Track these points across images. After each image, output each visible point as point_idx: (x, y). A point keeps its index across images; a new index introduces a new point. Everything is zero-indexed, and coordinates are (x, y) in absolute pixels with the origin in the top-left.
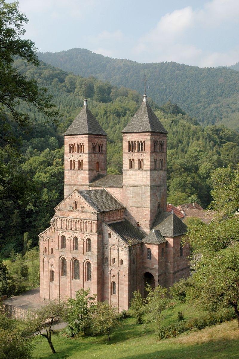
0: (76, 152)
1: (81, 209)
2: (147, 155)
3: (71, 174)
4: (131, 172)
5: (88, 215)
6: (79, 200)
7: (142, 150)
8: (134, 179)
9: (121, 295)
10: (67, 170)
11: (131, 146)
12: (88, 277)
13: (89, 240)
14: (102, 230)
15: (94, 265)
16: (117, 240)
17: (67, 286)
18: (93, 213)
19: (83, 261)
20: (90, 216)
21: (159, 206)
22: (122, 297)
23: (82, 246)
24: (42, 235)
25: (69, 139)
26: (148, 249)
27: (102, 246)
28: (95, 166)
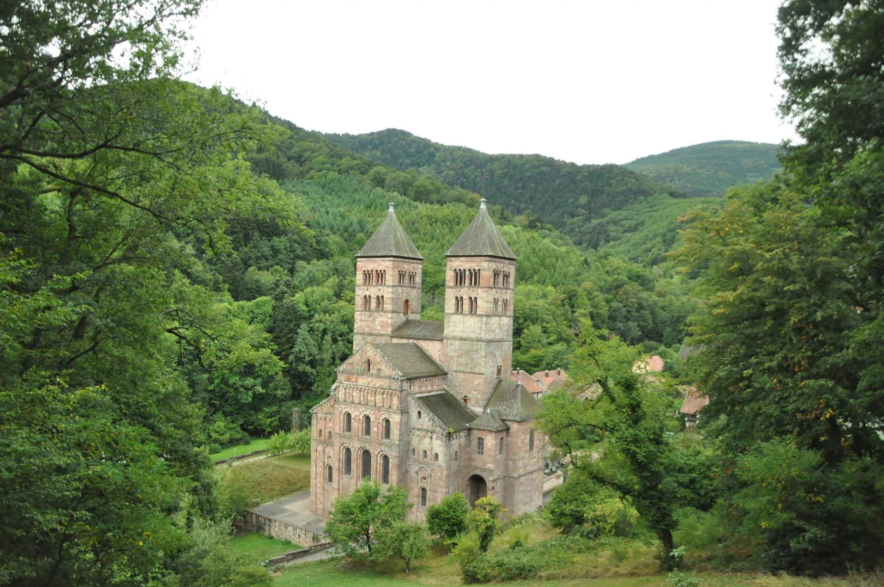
1: (376, 372)
4: (458, 318)
5: (387, 381)
7: (475, 284)
8: (460, 328)
11: (460, 277)
13: (388, 421)
14: (407, 406)
16: (431, 423)
21: (499, 371)
23: (375, 429)
24: (315, 411)
26: (479, 438)
27: (407, 430)
28: (402, 306)
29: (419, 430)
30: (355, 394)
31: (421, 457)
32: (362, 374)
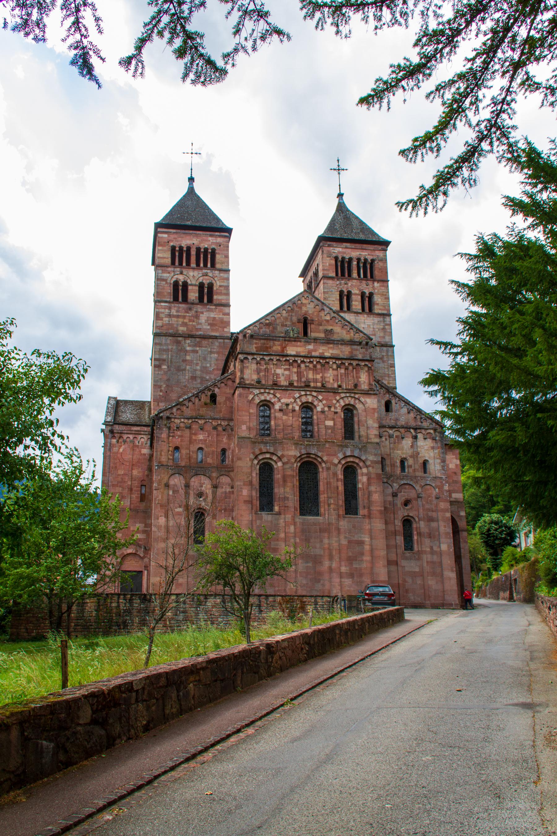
0: (193, 265)
3: (177, 311)
9: (431, 548)
10: (166, 302)
12: (351, 504)
13: (349, 411)
15: (373, 467)
17: (282, 535)
18: (360, 343)
19: (336, 461)
20: (351, 352)
22: (432, 552)
25: (172, 237)
29: (391, 427)
30: (279, 371)
31: (398, 470)
32: (296, 340)
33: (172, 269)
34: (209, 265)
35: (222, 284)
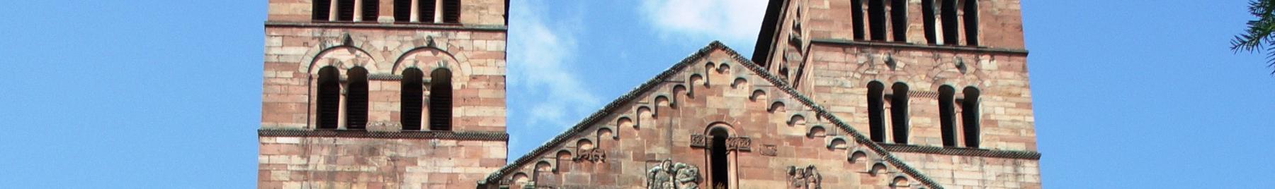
0: (386, 17)
2: (1000, 69)
3: (329, 161)
6: (763, 124)
33: (317, 32)
34: (438, 17)
35: (479, 71)
